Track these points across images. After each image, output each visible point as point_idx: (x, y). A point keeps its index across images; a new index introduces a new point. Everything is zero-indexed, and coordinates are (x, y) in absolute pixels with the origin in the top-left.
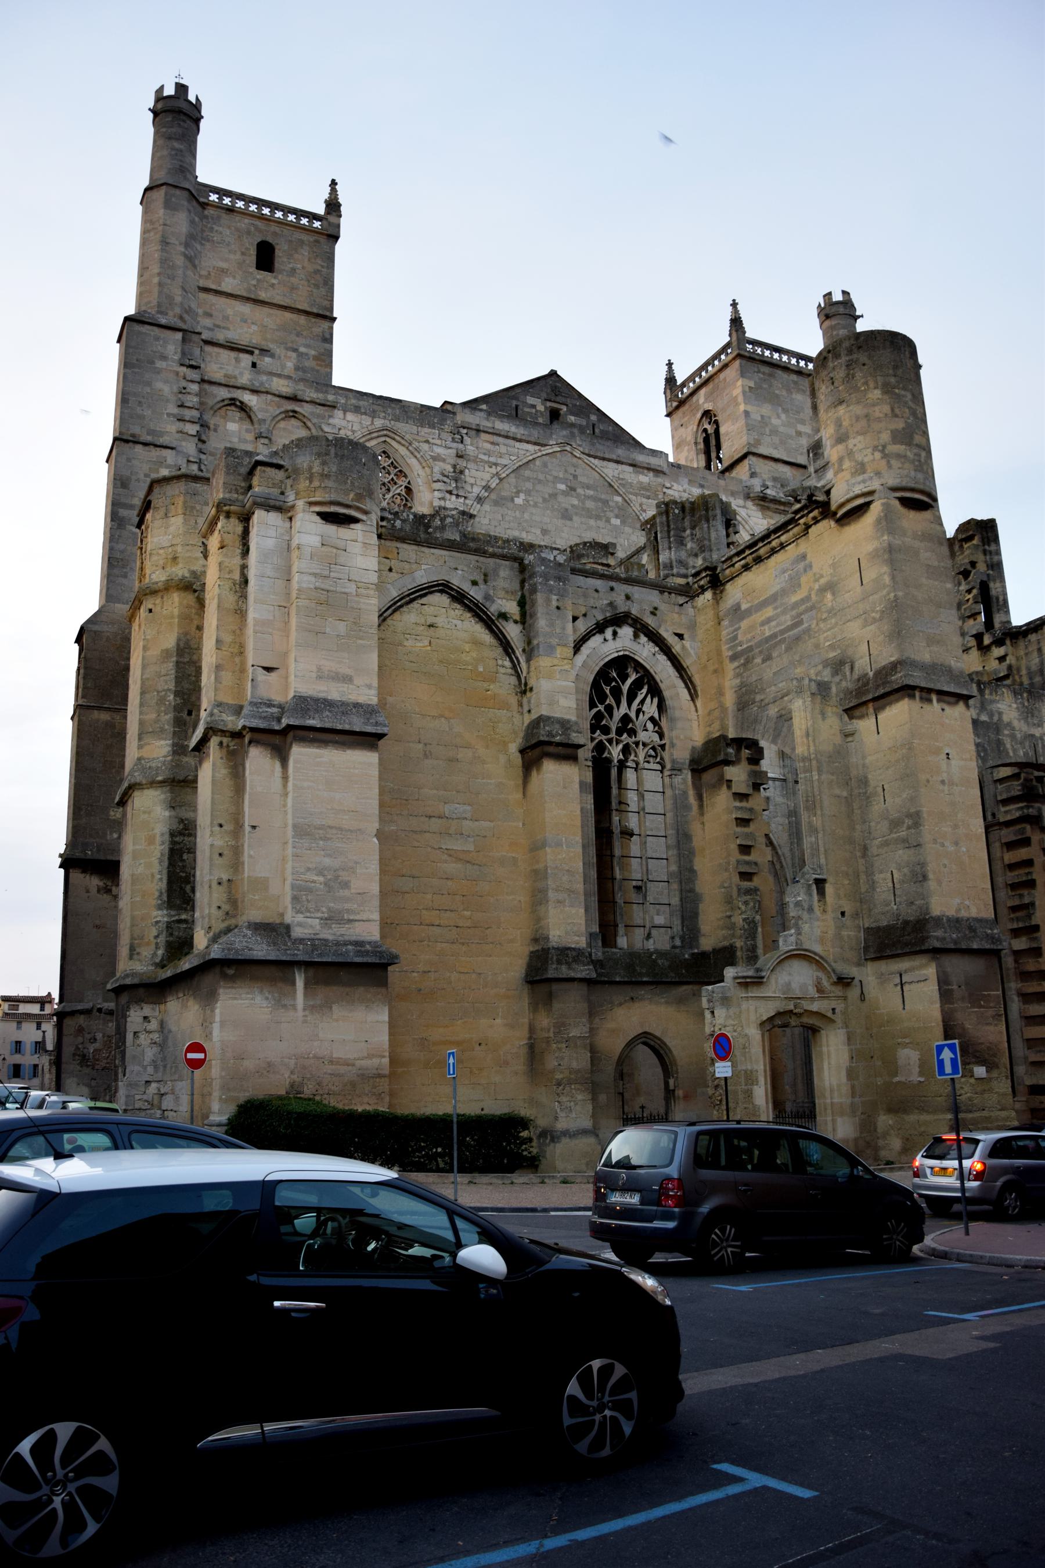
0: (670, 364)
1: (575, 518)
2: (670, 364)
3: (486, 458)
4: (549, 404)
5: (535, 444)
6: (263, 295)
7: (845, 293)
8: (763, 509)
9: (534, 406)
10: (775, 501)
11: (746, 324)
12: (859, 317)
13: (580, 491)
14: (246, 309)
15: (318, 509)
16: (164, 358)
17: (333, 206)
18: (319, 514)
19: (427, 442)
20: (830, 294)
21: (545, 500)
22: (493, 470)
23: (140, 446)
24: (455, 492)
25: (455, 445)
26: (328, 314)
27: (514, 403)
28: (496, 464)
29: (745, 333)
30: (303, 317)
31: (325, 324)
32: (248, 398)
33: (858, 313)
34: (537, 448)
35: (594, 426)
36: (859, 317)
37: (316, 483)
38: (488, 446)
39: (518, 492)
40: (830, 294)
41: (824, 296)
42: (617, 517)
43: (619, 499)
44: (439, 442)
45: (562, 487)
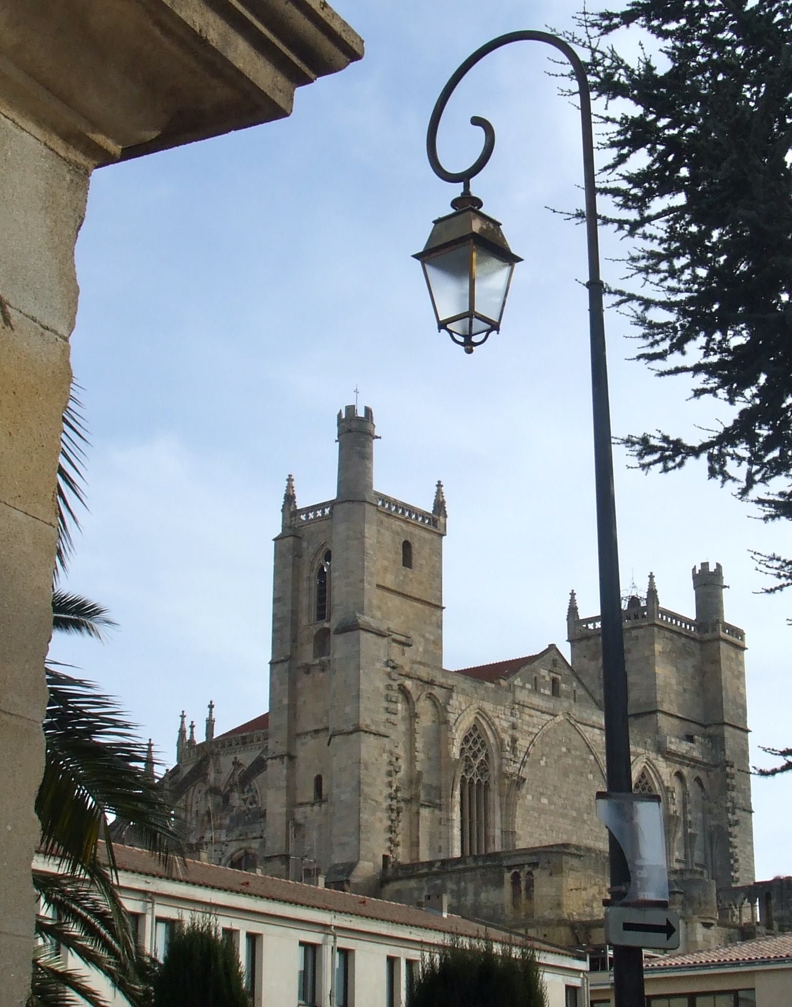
0: (573, 594)
1: (571, 775)
2: (573, 594)
3: (525, 728)
4: (552, 674)
5: (552, 715)
6: (407, 590)
7: (718, 565)
8: (666, 759)
9: (544, 677)
10: (675, 754)
11: (660, 595)
12: (725, 587)
13: (573, 752)
14: (397, 601)
15: (704, 921)
16: (379, 660)
17: (440, 505)
18: (702, 923)
19: (498, 717)
20: (707, 564)
21: (555, 760)
22: (530, 739)
23: (372, 736)
24: (513, 759)
25: (511, 719)
26: (438, 604)
27: (535, 675)
28: (531, 733)
29: (658, 603)
30: (427, 607)
31: (438, 613)
32: (409, 684)
33: (725, 584)
34: (552, 717)
35: (575, 691)
36: (725, 587)
37: (703, 907)
38: (527, 718)
39: (543, 755)
40: (707, 564)
41: (703, 564)
42: (591, 772)
43: (592, 757)
44: (503, 717)
45: (564, 749)
